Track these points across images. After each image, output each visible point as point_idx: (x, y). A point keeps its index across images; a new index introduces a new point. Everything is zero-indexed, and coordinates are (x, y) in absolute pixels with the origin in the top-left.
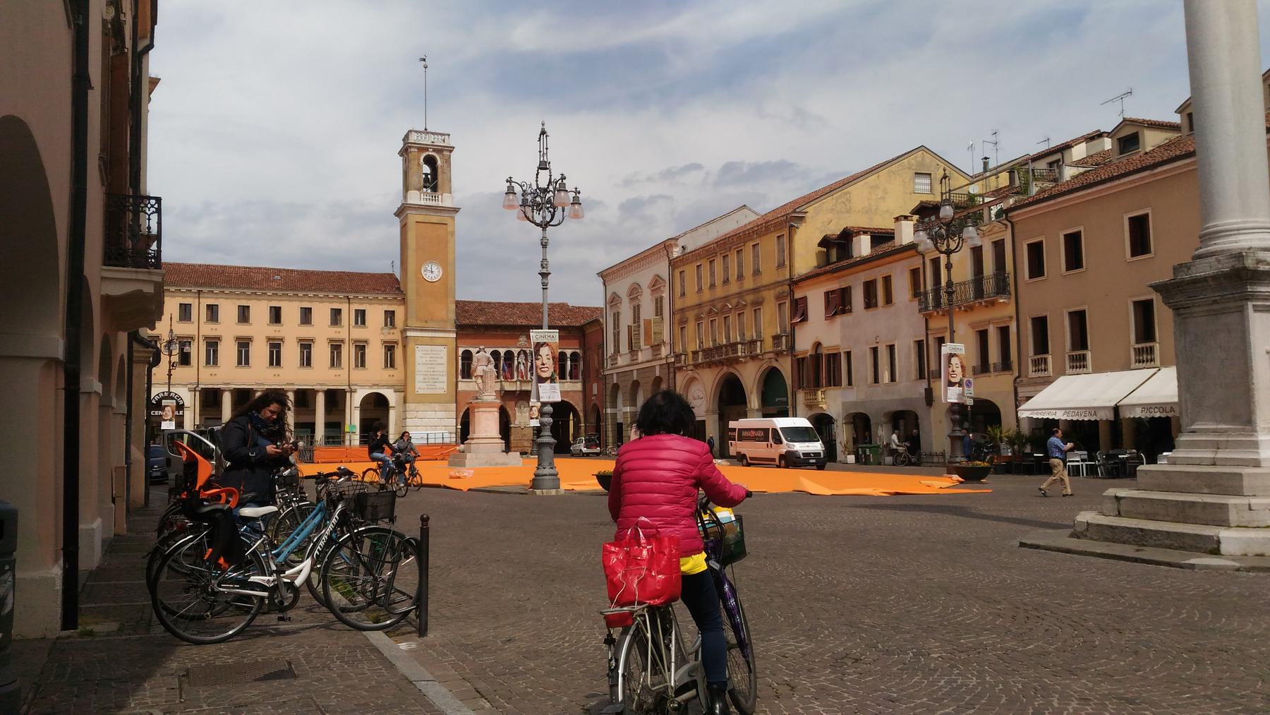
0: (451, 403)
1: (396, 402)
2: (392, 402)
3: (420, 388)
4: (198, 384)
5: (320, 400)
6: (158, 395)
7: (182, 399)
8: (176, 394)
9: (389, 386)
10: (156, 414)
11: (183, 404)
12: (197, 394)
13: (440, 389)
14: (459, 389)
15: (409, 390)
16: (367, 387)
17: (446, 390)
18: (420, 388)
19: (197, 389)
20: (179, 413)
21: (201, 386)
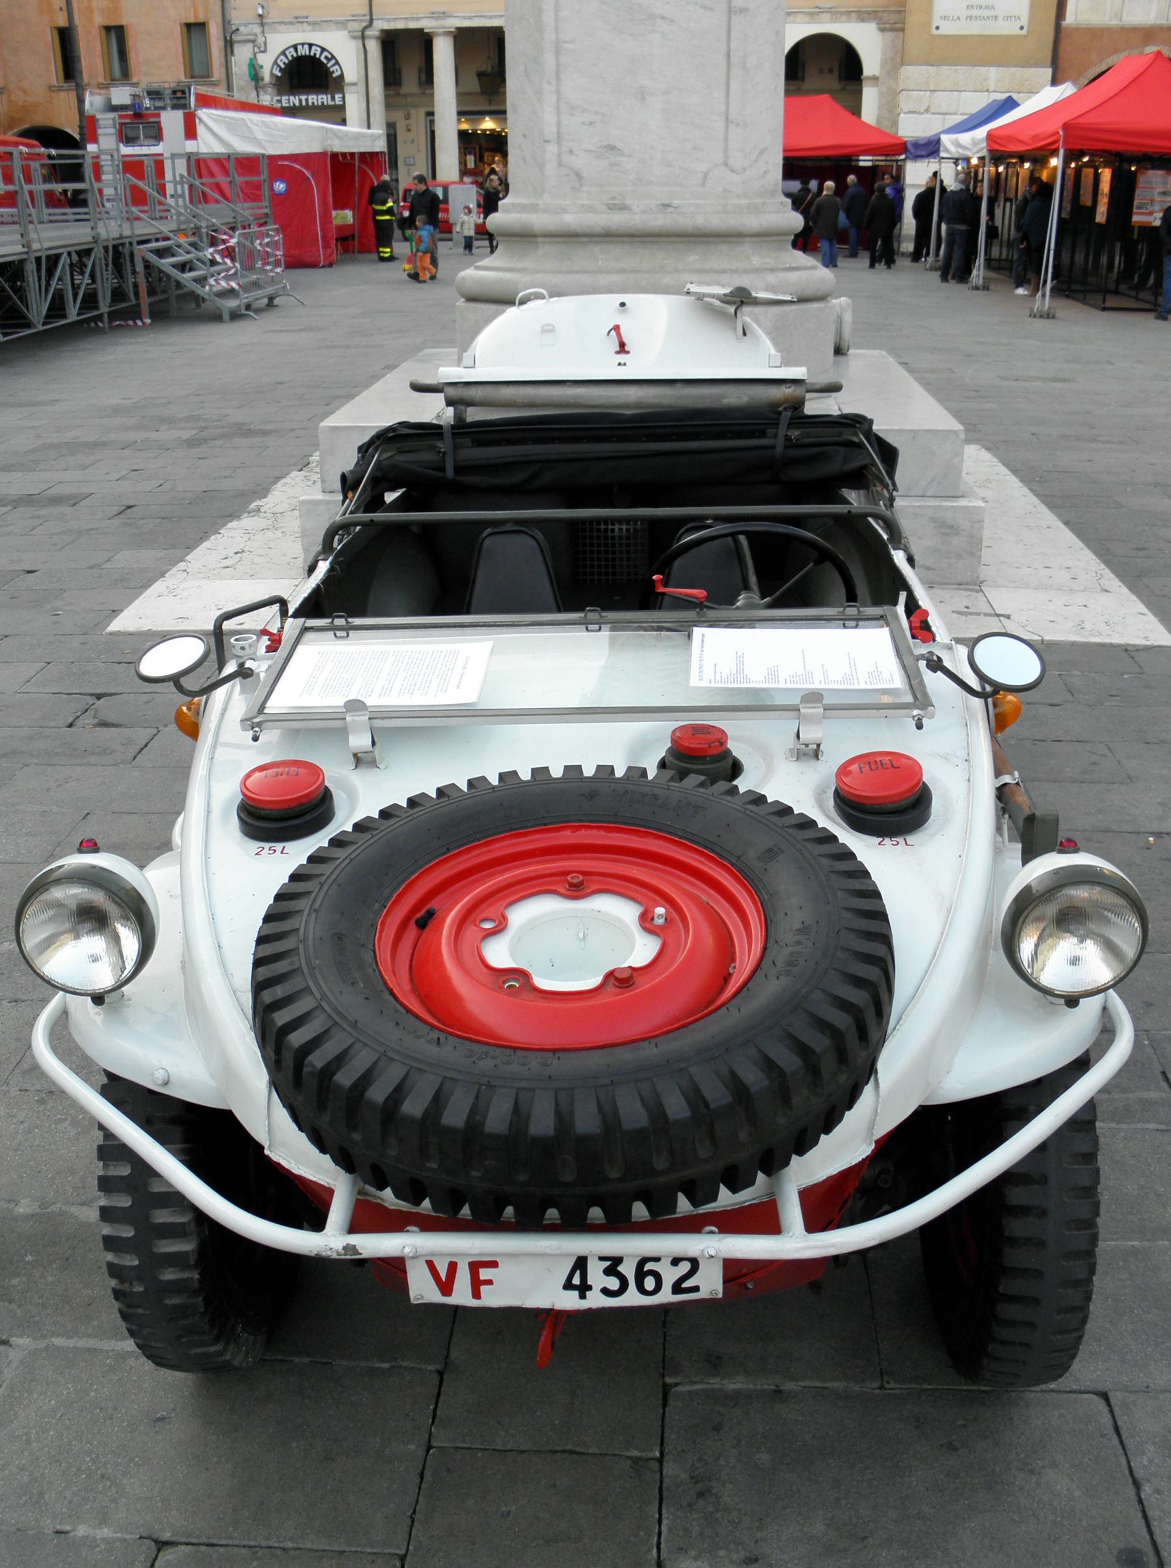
0: (1037, 64)
1: (883, 64)
2: (870, 66)
3: (945, 18)
4: (371, 21)
5: (444, 54)
6: (284, 53)
7: (337, 63)
8: (323, 50)
9: (863, 15)
10: (285, 104)
11: (342, 76)
12: (374, 48)
13: (1008, 18)
14: (1070, 19)
15: (913, 19)
16: (799, 17)
17: (1024, 21)
18: (945, 18)
19: (368, 33)
20: (333, 99)
21: (381, 25)
